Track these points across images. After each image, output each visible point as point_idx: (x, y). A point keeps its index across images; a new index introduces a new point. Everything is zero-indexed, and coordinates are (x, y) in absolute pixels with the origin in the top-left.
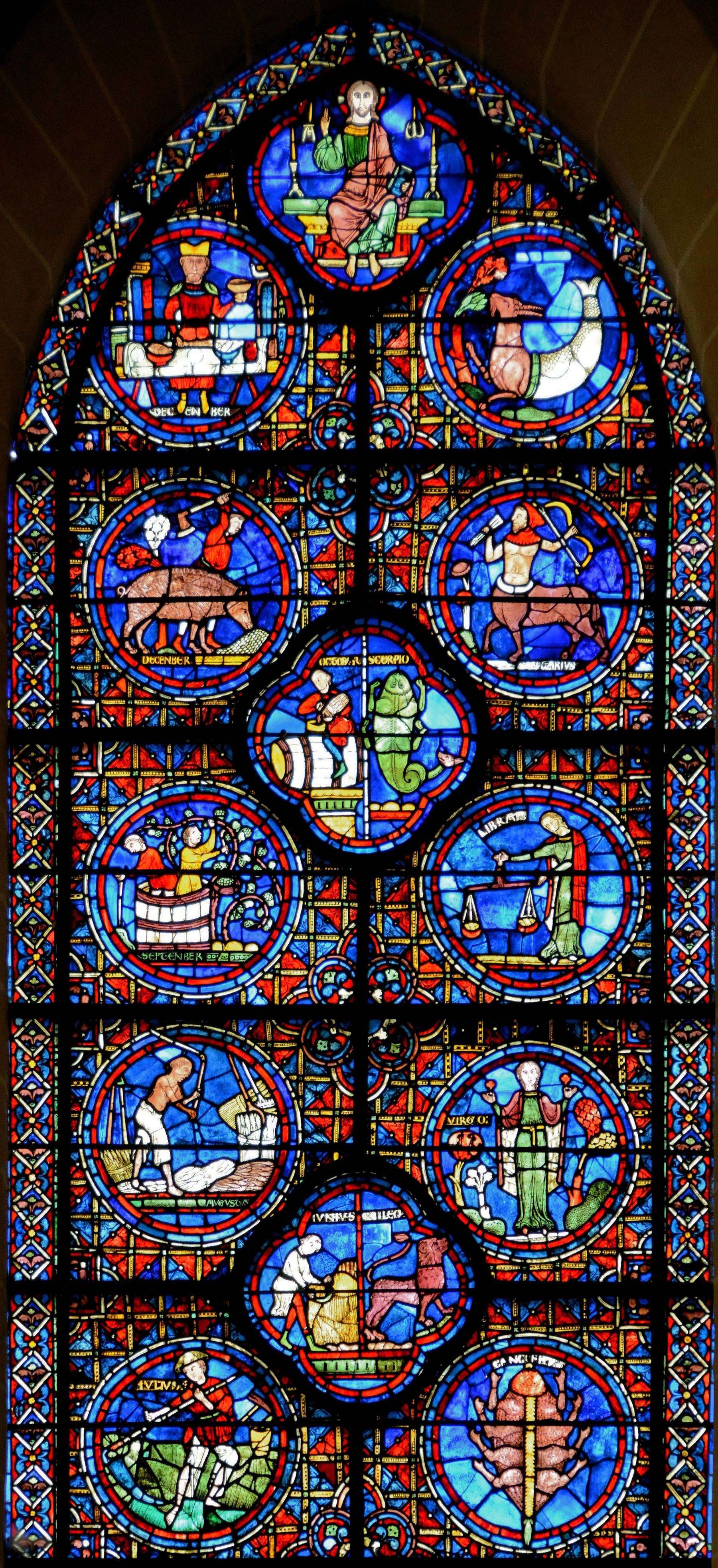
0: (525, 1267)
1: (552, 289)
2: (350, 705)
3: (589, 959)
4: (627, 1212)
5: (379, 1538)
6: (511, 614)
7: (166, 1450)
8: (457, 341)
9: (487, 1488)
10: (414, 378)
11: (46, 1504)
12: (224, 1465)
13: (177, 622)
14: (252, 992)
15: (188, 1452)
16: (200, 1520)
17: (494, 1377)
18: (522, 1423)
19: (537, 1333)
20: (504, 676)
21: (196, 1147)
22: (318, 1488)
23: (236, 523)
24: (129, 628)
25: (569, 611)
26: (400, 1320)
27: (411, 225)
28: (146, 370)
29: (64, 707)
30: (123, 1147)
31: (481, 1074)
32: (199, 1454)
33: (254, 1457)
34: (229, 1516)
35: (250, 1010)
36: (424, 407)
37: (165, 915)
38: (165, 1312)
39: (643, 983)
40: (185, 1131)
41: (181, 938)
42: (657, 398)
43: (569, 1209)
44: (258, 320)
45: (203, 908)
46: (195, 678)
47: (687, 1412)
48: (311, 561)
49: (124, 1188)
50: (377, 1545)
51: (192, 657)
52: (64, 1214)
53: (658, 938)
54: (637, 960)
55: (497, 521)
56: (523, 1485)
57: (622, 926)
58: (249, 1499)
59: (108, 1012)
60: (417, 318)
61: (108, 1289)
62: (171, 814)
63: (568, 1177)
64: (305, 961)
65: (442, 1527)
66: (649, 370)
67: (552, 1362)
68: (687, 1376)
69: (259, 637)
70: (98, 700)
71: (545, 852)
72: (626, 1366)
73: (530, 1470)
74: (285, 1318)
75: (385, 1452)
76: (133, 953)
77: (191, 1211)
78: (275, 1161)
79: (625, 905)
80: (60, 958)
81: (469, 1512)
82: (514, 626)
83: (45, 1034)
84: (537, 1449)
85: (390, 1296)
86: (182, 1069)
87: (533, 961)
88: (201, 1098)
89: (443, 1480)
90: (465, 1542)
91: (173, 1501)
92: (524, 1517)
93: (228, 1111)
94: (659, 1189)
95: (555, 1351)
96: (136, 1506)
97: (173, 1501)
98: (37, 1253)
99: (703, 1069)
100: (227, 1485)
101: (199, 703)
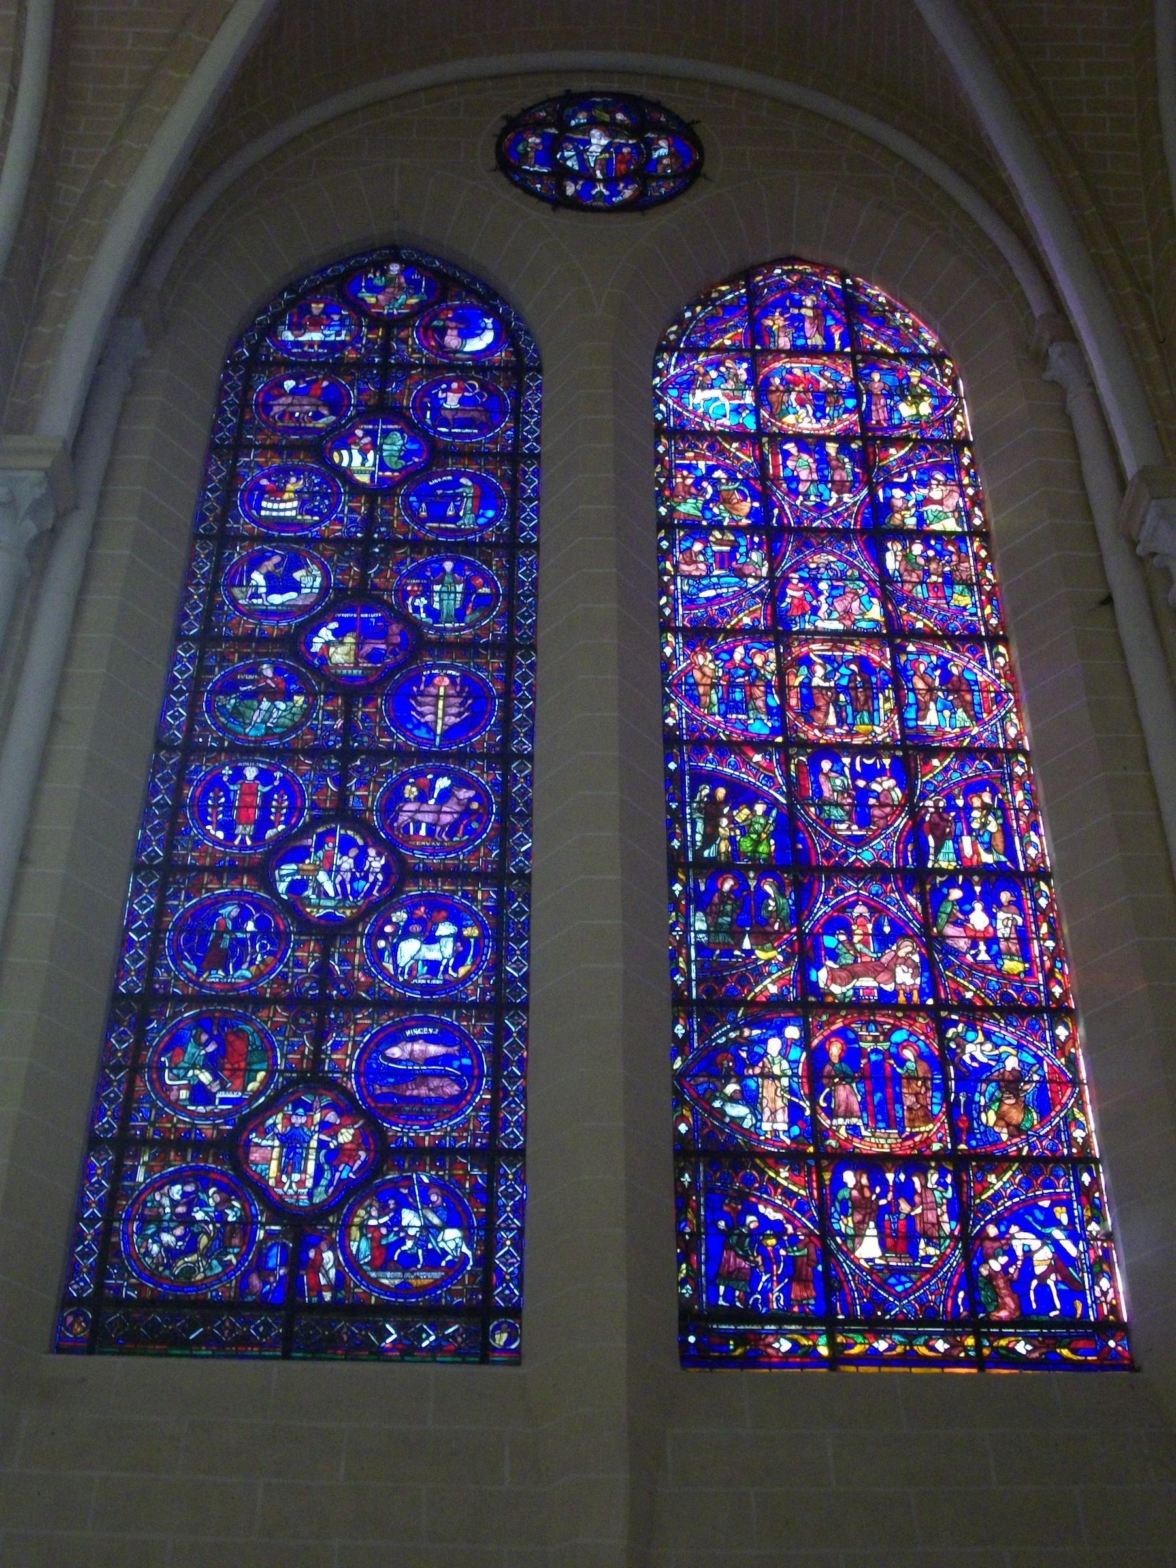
0: (442, 636)
6: (449, 415)
12: (278, 709)
15: (260, 703)
25: (475, 414)
27: (413, 301)
32: (265, 704)
34: (278, 730)
37: (276, 506)
41: (282, 514)
45: (295, 504)
55: (444, 386)
56: (436, 722)
61: (227, 639)
62: (284, 473)
67: (454, 673)
73: (440, 713)
80: (222, 520)
82: (450, 417)
84: (445, 707)
86: (276, 559)
93: (297, 575)
100: (280, 717)
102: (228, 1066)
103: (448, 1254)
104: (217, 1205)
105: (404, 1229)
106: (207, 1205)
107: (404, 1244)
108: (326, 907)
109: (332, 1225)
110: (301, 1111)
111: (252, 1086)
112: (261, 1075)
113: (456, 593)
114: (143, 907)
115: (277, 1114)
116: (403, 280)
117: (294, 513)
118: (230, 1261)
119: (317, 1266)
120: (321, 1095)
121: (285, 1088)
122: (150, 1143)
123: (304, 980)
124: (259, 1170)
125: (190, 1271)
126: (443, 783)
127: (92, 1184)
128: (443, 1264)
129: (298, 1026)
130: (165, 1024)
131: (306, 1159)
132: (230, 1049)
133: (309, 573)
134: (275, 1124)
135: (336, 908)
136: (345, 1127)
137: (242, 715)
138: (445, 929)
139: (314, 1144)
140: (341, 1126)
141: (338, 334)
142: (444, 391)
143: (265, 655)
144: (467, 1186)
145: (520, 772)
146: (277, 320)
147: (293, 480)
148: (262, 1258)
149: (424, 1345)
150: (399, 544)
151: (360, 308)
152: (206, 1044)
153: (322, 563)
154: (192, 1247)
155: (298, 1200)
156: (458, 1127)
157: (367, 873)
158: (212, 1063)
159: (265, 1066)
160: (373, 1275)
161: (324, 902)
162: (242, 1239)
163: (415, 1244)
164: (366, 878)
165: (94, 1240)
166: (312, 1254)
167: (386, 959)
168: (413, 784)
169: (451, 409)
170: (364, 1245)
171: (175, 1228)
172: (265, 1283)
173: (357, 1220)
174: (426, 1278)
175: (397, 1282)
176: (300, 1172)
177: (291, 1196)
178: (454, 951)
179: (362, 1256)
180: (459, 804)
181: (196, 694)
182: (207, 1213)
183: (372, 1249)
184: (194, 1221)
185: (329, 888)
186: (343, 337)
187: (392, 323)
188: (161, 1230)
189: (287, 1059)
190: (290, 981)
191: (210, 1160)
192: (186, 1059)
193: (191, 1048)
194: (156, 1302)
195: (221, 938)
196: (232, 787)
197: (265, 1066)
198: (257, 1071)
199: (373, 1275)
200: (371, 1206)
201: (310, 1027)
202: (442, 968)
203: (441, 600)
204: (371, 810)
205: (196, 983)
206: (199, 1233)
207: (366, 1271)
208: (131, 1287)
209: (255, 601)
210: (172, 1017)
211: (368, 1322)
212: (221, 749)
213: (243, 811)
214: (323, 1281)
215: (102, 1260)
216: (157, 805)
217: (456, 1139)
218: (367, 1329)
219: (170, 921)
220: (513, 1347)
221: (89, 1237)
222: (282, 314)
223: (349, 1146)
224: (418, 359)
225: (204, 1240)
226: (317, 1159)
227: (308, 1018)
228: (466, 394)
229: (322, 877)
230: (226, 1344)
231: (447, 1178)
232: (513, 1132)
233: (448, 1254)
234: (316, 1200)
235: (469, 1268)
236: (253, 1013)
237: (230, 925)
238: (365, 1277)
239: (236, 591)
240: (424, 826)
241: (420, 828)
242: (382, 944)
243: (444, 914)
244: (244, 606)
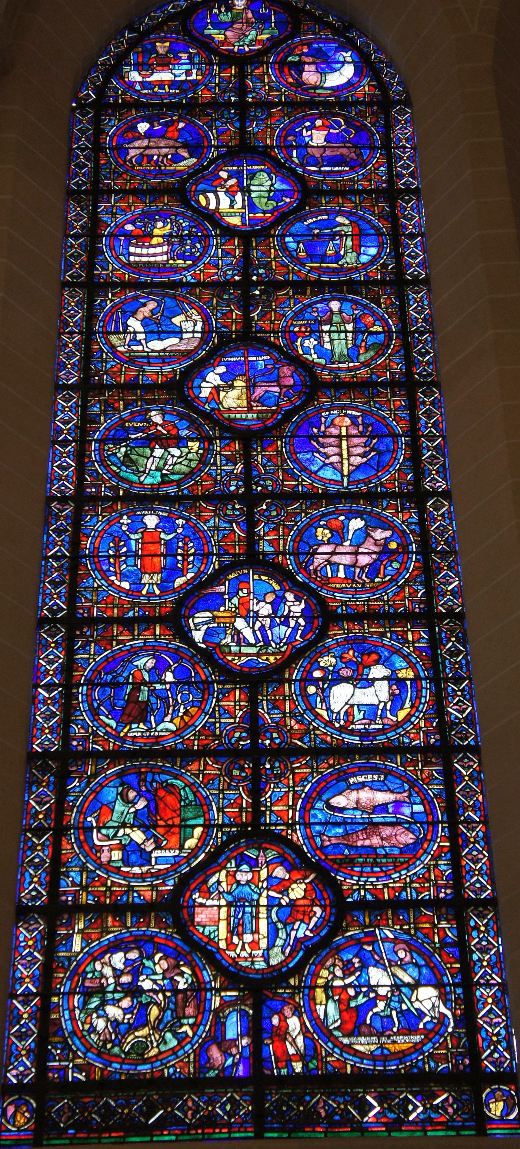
0: (337, 377)
1: (330, 54)
2: (238, 182)
3: (363, 264)
4: (390, 355)
5: (261, 486)
6: (317, 153)
7: (140, 450)
8: (286, 70)
9: (321, 463)
10: (266, 80)
11: (71, 474)
12: (173, 456)
13: (153, 156)
14: (189, 278)
15: (152, 450)
16: (159, 479)
17: (323, 419)
18: (340, 437)
19: (347, 402)
20: (315, 172)
21: (159, 333)
22: (226, 465)
23: (181, 125)
24: (129, 157)
25: (344, 151)
26: (270, 398)
27: (264, 37)
28: (140, 79)
29: (96, 181)
30: (119, 333)
31: (310, 306)
32: (158, 452)
33: (190, 452)
35: (188, 284)
36: (271, 89)
38: (141, 395)
39: (391, 273)
40: (154, 327)
41: (152, 259)
42: (382, 86)
43: (359, 354)
44: (192, 63)
45: (165, 248)
46: (161, 173)
47: (431, 432)
48: (218, 136)
49: (119, 349)
50: (259, 489)
51: (160, 167)
52: (87, 358)
53: (398, 257)
54: (388, 265)
55: (308, 124)
56: (341, 463)
57: (379, 253)
58: (186, 470)
59: (114, 285)
60: (267, 63)
61: (110, 387)
62: (149, 217)
63: (358, 342)
64: (216, 266)
65: (297, 480)
66: (376, 75)
67: (354, 413)
68: (429, 417)
69: (194, 160)
70: (113, 180)
71: (338, 229)
72: (395, 414)
73: (345, 455)
74: (207, 398)
75: (263, 450)
76: (128, 265)
77: (156, 357)
78: (201, 338)
79: (380, 247)
81: (311, 474)
82: (318, 156)
83: (81, 294)
85: (264, 389)
86: (152, 305)
87: (335, 265)
88: (162, 315)
89: (296, 461)
90: (310, 487)
91: (144, 472)
92: (342, 475)
94: (406, 347)
95: (356, 408)
96: (122, 474)
97: (144, 472)
98: (71, 374)
99: (426, 303)
100: (175, 464)
101: (163, 182)
102: (161, 823)
103: (426, 1015)
104: (165, 972)
105: (372, 988)
106: (155, 973)
107: (376, 1006)
108: (247, 655)
109: (294, 988)
110: (245, 867)
111: (190, 843)
112: (198, 831)
113: (346, 332)
114: (51, 662)
115: (220, 871)
116: (250, 15)
117: (165, 258)
118: (186, 1033)
119: (282, 1034)
120: (265, 850)
121: (225, 844)
122: (86, 909)
123: (234, 730)
124: (207, 933)
125: (141, 1047)
126: (356, 524)
127: (23, 958)
128: (421, 1026)
129: (232, 777)
130: (88, 783)
131: (257, 918)
132: (162, 806)
133: (188, 318)
134: (219, 882)
135: (258, 655)
136: (295, 882)
137: (135, 463)
138: (378, 671)
139: (263, 901)
140: (291, 881)
141: (188, 73)
142: (308, 129)
143: (153, 402)
144: (436, 940)
145: (437, 509)
146: (121, 59)
147: (160, 224)
148: (220, 1025)
149: (411, 1118)
150: (280, 285)
151: (207, 46)
152: (134, 803)
153: (201, 308)
154: (142, 1021)
155: (253, 963)
156: (419, 878)
157: (287, 617)
158: (142, 822)
159: (201, 821)
160: (346, 1041)
161: (244, 650)
162: (198, 1007)
163: (388, 1005)
164: (286, 623)
165: (30, 1018)
166: (275, 1020)
167: (319, 705)
168: (325, 527)
169: (318, 147)
170: (332, 1009)
171: (120, 1000)
172: (226, 1054)
173: (320, 982)
174: (404, 1042)
175: (373, 1048)
176: (253, 933)
177: (246, 959)
178: (390, 695)
179: (330, 1021)
180: (376, 544)
181: (83, 443)
182: (155, 982)
183: (340, 1012)
184: (141, 991)
185: (248, 634)
186: (194, 77)
187: (243, 61)
188: (104, 1003)
189: (224, 813)
190: (218, 732)
191: (152, 925)
192: (114, 818)
193: (119, 807)
194: (107, 1085)
195: (139, 690)
196: (132, 536)
197: (201, 821)
198: (194, 827)
199: (346, 1041)
200: (334, 965)
201: (244, 779)
202: (379, 712)
203: (331, 341)
204: (284, 554)
205: (117, 737)
206: (148, 1004)
207: (337, 1038)
208: (78, 1068)
209: (135, 348)
210: (95, 775)
211: (347, 1093)
212: (116, 499)
213: (147, 560)
214: (291, 1051)
215: (42, 1041)
216: (55, 557)
217: (418, 891)
218: (345, 1103)
219: (82, 675)
220: (512, 1117)
221: (25, 1016)
222: (126, 54)
223: (301, 902)
224: (276, 96)
225: (154, 1012)
226: (269, 917)
227: (242, 769)
228: (332, 131)
229: (240, 623)
230: (190, 1127)
231: (413, 932)
232: (478, 881)
233: (426, 1015)
234: (273, 962)
235: (450, 1030)
236: (182, 767)
237: (146, 677)
238: (338, 1044)
239: (114, 339)
240: (341, 568)
241: (338, 571)
242: (312, 690)
243: (374, 657)
244: (122, 353)
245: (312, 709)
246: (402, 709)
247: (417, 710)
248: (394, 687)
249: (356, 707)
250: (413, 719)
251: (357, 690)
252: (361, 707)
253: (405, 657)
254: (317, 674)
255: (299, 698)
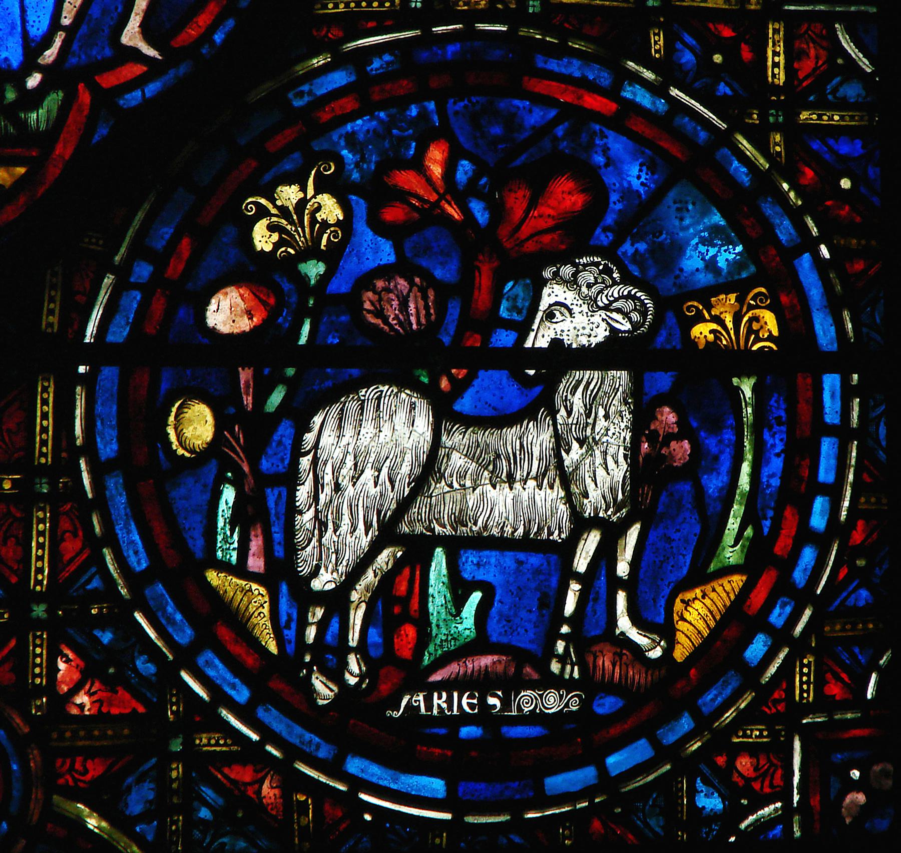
243: (566, 196)
245: (181, 565)
246: (700, 576)
247: (783, 587)
248: (668, 417)
249: (439, 559)
250: (757, 648)
251: (456, 437)
252: (469, 559)
253: (743, 210)
254: (226, 313)
255: (114, 484)
